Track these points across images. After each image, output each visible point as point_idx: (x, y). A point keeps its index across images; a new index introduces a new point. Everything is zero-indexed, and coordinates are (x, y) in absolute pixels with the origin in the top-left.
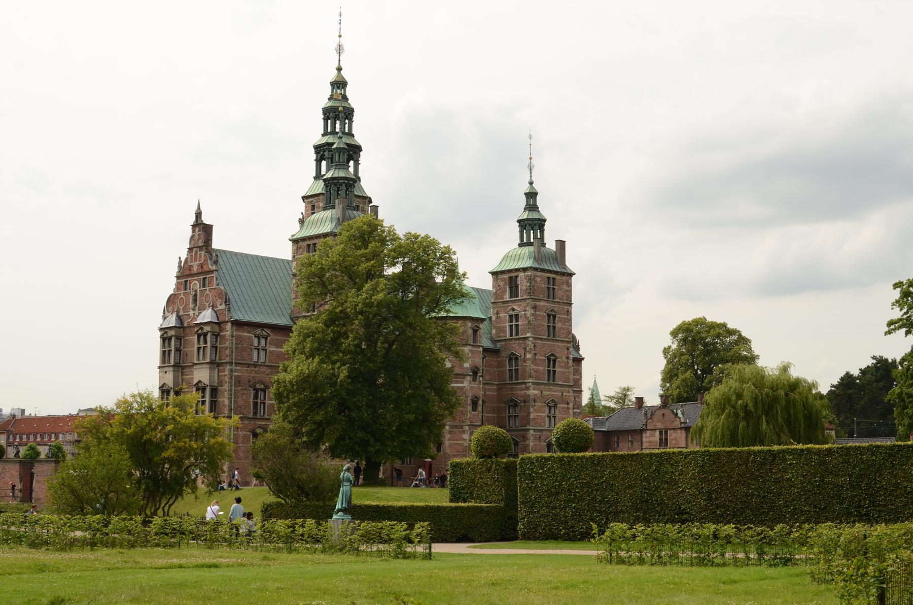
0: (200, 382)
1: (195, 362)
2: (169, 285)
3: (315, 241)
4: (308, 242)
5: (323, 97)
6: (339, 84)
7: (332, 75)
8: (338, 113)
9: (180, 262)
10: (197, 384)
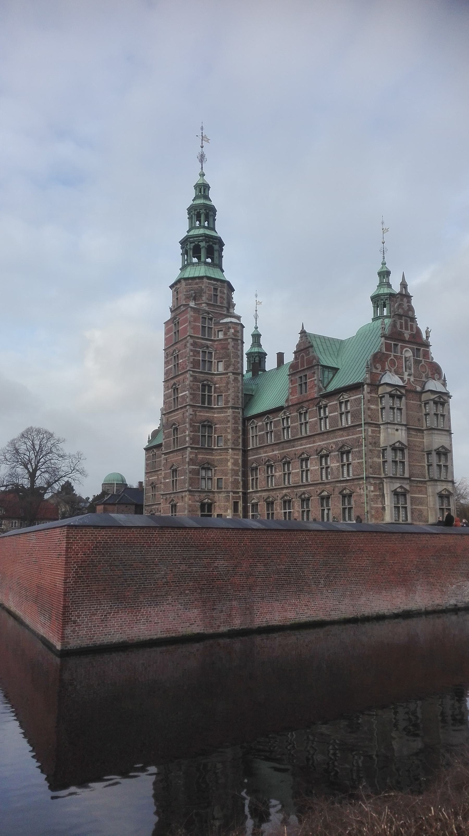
0: (443, 447)
6: (203, 189)
8: (202, 212)
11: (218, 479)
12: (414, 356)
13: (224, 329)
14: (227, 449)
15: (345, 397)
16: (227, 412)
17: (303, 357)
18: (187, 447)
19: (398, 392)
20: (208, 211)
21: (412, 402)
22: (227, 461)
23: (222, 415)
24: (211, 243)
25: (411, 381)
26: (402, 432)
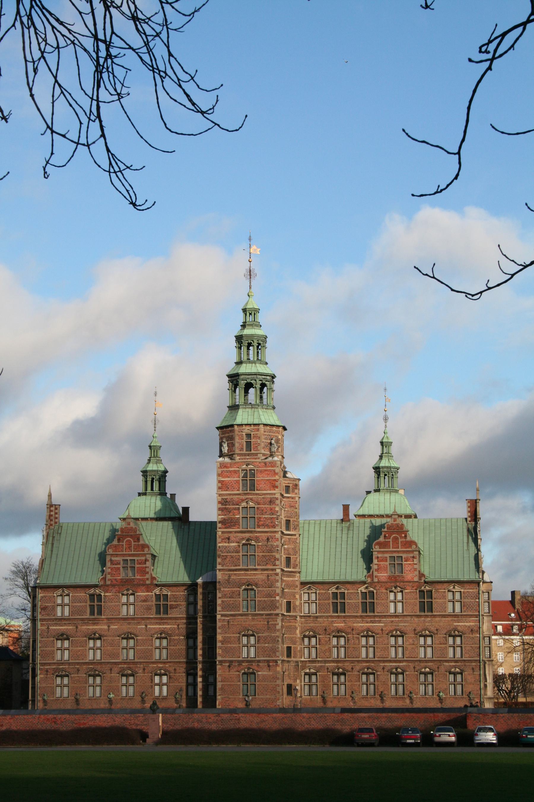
11: (287, 647)
13: (291, 485)
14: (296, 617)
15: (456, 587)
16: (294, 576)
17: (396, 539)
18: (277, 615)
22: (296, 628)
23: (291, 579)
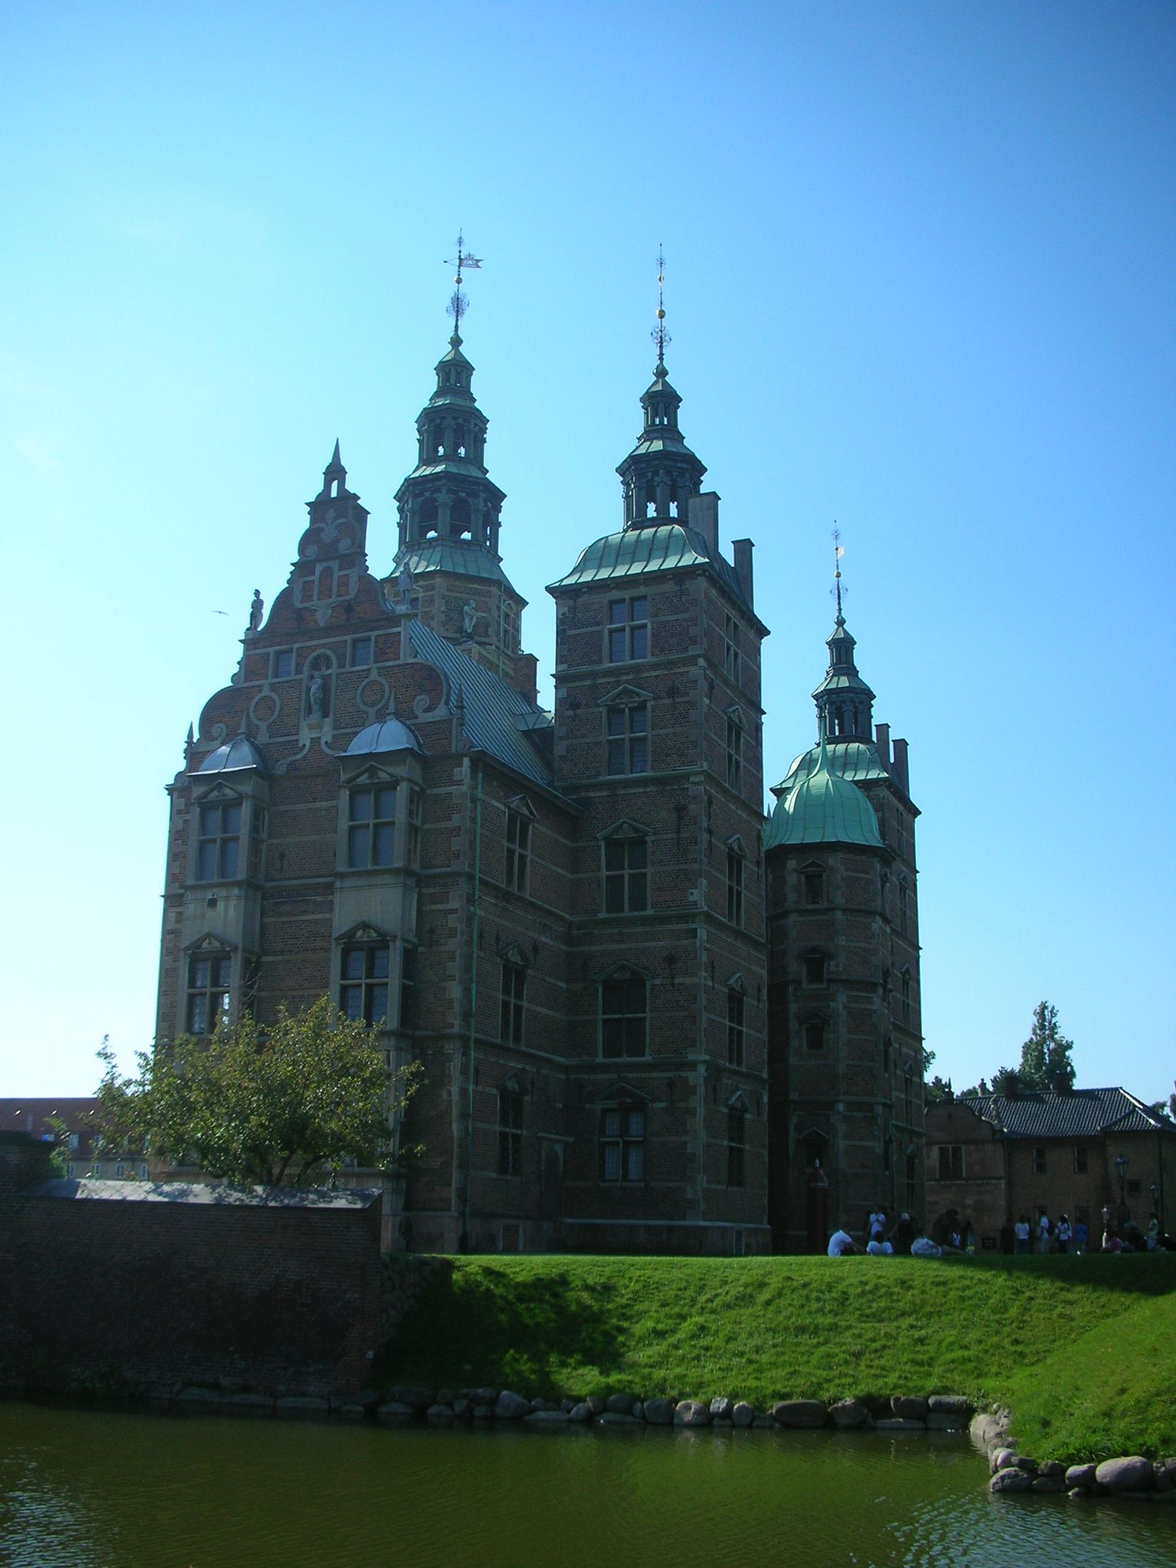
0: (365, 926)
1: (342, 868)
2: (220, 665)
3: (642, 590)
4: (615, 595)
5: (423, 389)
6: (455, 373)
7: (444, 351)
8: (453, 421)
9: (257, 605)
10: (350, 934)
12: (342, 665)
19: (228, 791)
20: (438, 421)
21: (318, 805)
24: (428, 494)
25: (323, 742)
26: (226, 907)
